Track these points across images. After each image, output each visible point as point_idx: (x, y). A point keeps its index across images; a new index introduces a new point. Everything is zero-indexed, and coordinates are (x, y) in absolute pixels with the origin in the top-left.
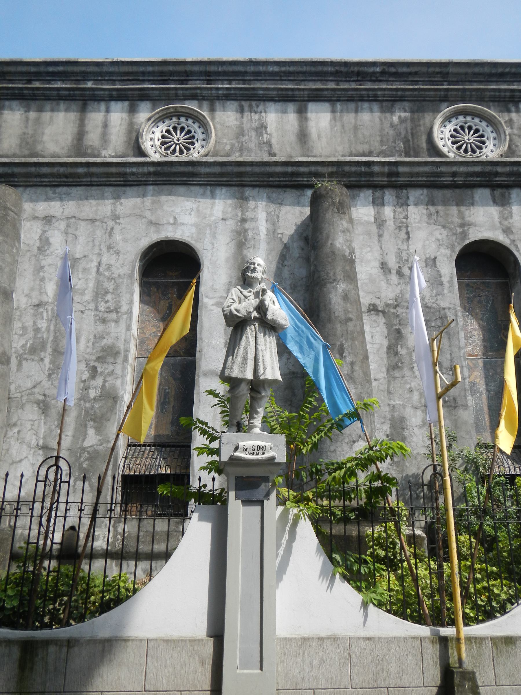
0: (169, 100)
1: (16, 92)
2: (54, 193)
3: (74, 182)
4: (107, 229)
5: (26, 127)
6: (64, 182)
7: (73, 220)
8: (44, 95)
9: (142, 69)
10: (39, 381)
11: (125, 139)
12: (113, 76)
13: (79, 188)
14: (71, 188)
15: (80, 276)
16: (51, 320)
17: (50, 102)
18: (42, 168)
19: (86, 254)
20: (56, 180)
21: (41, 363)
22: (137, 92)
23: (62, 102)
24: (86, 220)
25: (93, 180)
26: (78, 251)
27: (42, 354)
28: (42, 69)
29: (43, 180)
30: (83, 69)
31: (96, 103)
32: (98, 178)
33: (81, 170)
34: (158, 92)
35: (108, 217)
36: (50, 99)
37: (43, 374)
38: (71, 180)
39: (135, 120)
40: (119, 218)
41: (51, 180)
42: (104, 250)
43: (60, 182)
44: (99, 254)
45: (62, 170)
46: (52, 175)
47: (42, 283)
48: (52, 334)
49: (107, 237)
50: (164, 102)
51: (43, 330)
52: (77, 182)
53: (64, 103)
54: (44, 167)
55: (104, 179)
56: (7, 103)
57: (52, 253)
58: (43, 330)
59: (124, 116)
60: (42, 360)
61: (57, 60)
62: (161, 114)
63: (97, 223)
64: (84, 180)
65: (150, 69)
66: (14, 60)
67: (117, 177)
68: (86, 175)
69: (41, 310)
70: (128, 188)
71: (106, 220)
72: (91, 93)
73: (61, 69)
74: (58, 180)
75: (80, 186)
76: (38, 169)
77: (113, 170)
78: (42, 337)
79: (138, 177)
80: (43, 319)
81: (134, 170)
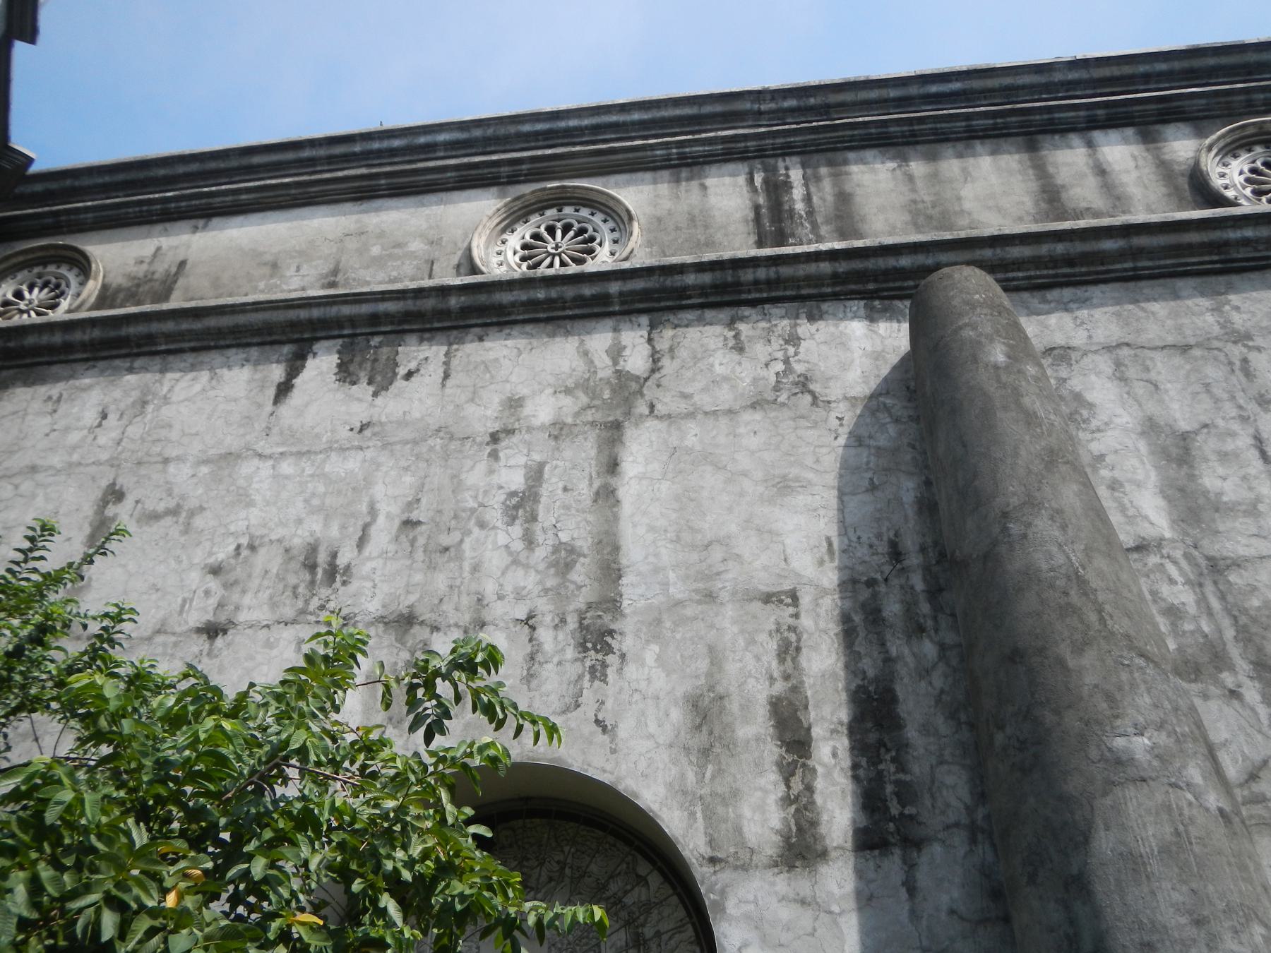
0: (1230, 115)
1: (873, 131)
2: (1045, 301)
3: (1088, 274)
4: (1231, 363)
5: (914, 190)
6: (1065, 275)
7: (1125, 352)
8: (935, 132)
9: (1142, 69)
10: (1257, 758)
11: (1164, 190)
12: (1075, 90)
13: (1103, 287)
14: (1084, 288)
15: (1221, 471)
16: (1201, 585)
17: (950, 144)
18: (1007, 248)
19: (1204, 418)
20: (1045, 272)
21: (1236, 703)
22: (1154, 107)
23: (977, 142)
24: (1163, 348)
25: (1140, 264)
26: (1178, 415)
27: (1228, 679)
28: (913, 90)
29: (1011, 275)
30: (1007, 81)
31: (1057, 137)
32: (1151, 259)
33: (1109, 245)
34: (1203, 101)
35: (1217, 338)
36: (947, 140)
37: (1259, 737)
38: (1084, 269)
39: (1167, 157)
40: (1248, 337)
41: (1032, 273)
42: (1252, 407)
43: (1056, 276)
44: (1244, 419)
45: (1060, 248)
46: (1036, 262)
47: (1116, 494)
48: (1226, 623)
49: (1243, 380)
50: (1218, 121)
51: (1192, 609)
52: (1097, 273)
53: (982, 144)
54: (1015, 245)
55: (1169, 262)
56: (851, 155)
57: (1106, 424)
58: (1192, 609)
59: (1136, 153)
60: (1234, 694)
61: (946, 70)
62: (1228, 140)
63: (1197, 352)
64: (1118, 266)
65: (1162, 67)
66: (852, 80)
67: (1202, 255)
68: (1121, 255)
69: (1153, 560)
70: (1235, 278)
71: (1216, 344)
72: (1046, 117)
73: (956, 86)
74: (1051, 272)
75: (1105, 281)
76: (998, 251)
77: (1194, 237)
78: (1199, 630)
79: (1256, 250)
80: (1172, 582)
81: (1249, 233)
